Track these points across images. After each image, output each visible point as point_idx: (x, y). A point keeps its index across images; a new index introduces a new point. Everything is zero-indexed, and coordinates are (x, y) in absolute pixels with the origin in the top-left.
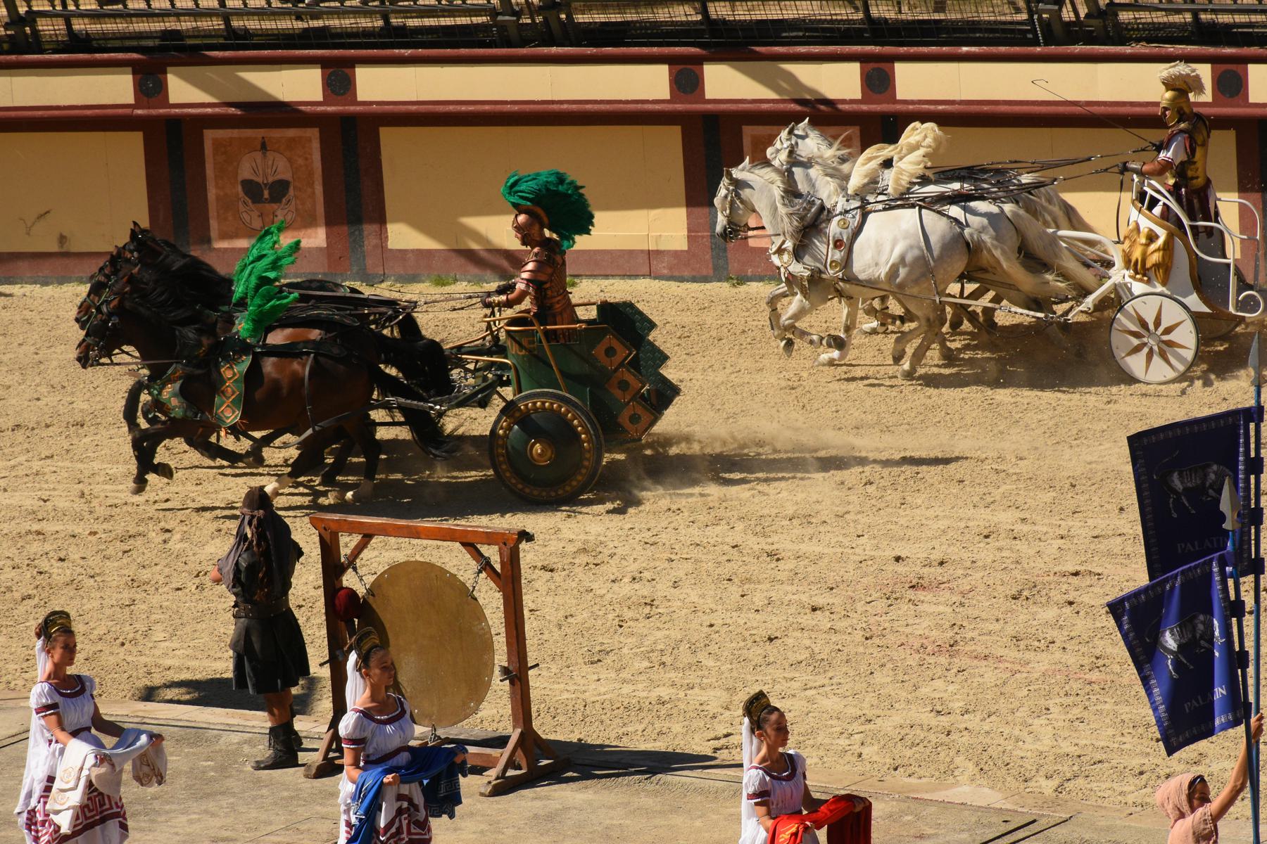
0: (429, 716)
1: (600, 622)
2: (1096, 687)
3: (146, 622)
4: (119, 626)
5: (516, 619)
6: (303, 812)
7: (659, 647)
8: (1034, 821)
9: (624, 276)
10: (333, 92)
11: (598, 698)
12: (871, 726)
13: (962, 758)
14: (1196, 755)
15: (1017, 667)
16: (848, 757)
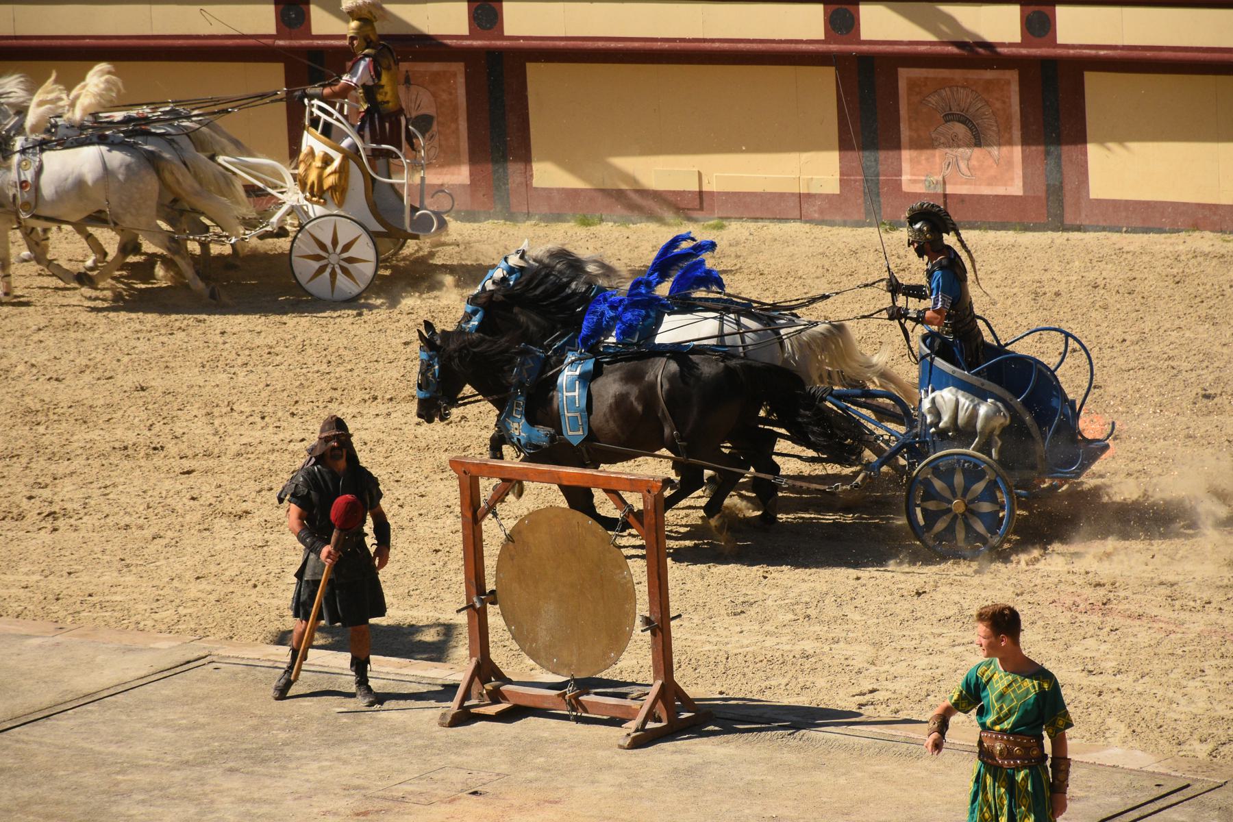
0: (568, 666)
3: (279, 563)
4: (251, 568)
5: (659, 569)
7: (804, 600)
8: (1188, 786)
13: (1114, 719)
15: (1172, 627)
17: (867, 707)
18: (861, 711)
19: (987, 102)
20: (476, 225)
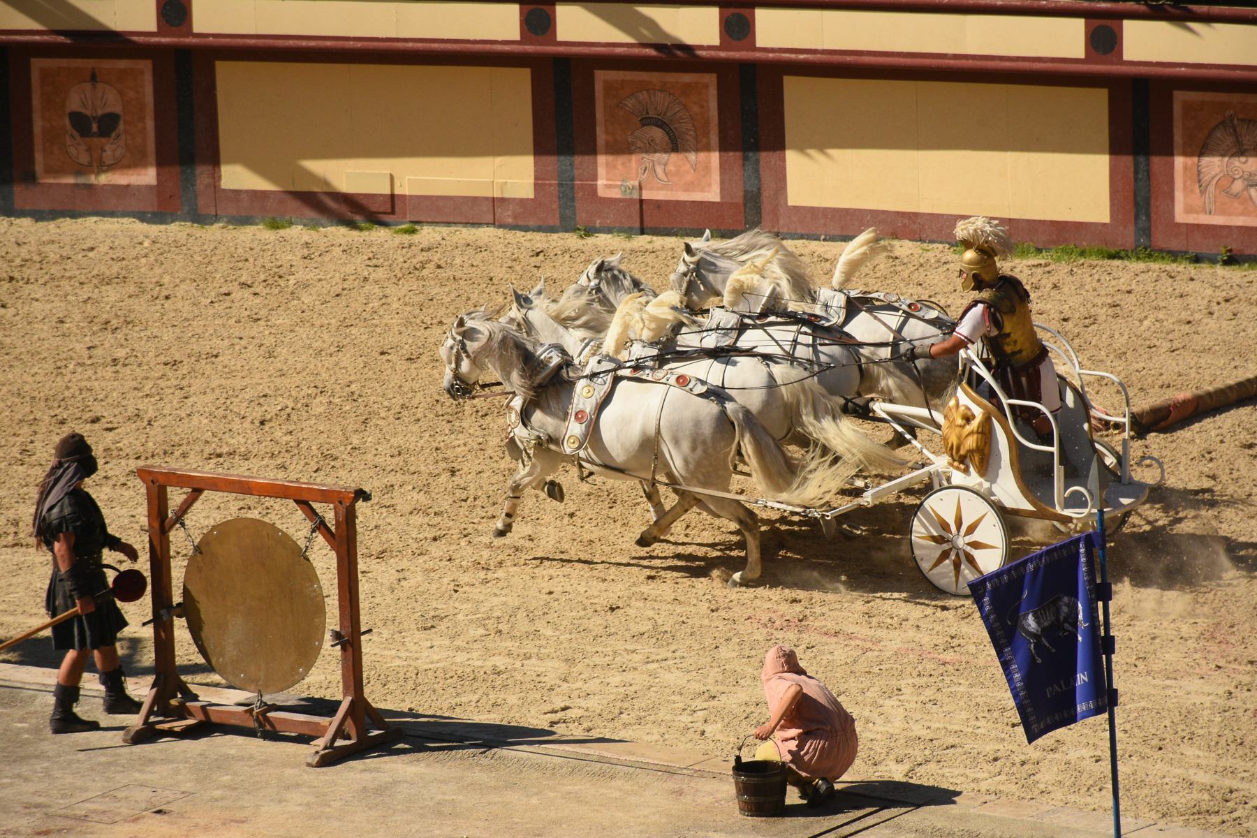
1: (434, 586)
2: (950, 668)
5: (349, 582)
6: (122, 779)
7: (495, 614)
9: (467, 224)
10: (167, 21)
11: (430, 666)
12: (715, 703)
14: (1053, 741)
15: (868, 645)
16: (690, 734)
17: (559, 725)
18: (553, 729)
19: (685, 106)
20: (162, 227)
